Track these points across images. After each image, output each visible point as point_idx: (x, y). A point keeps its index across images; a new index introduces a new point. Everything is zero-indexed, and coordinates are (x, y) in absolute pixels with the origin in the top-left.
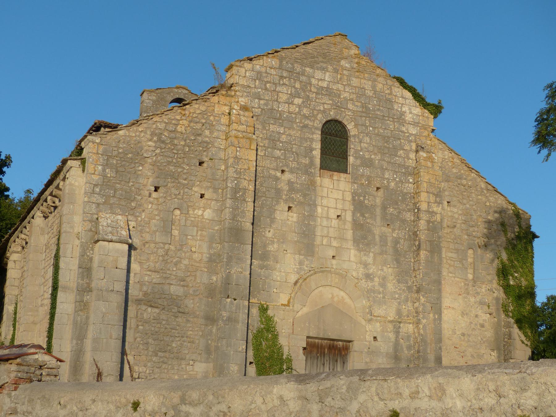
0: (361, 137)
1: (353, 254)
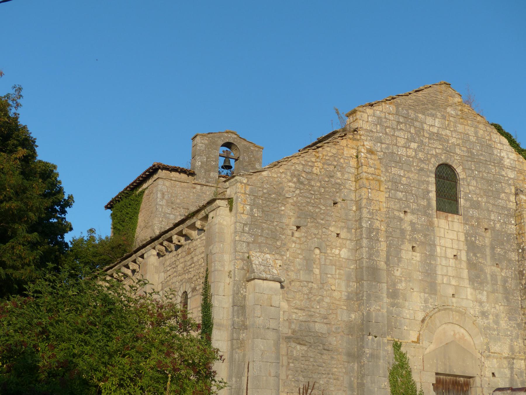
0: (469, 180)
1: (469, 292)
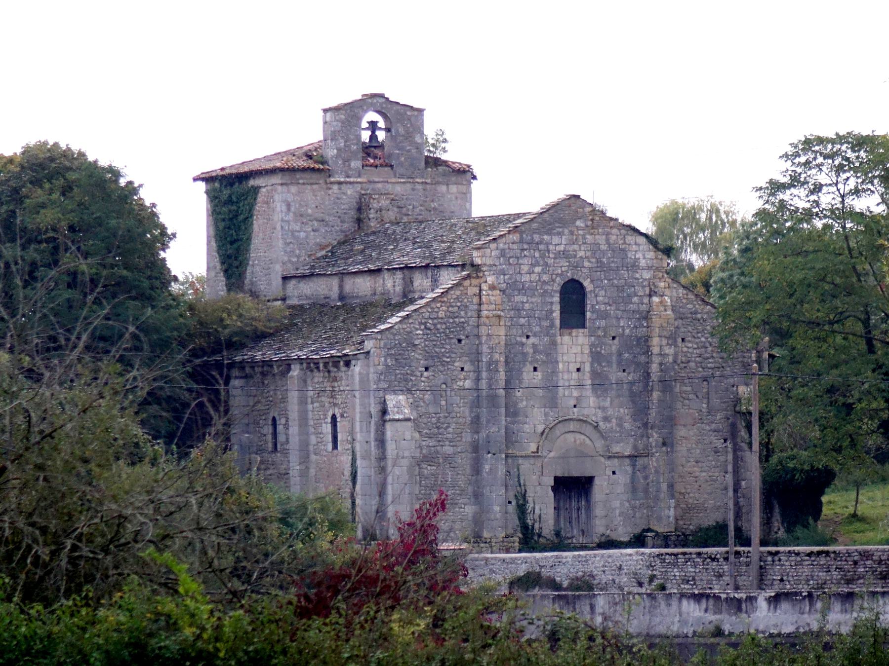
1: (592, 401)
